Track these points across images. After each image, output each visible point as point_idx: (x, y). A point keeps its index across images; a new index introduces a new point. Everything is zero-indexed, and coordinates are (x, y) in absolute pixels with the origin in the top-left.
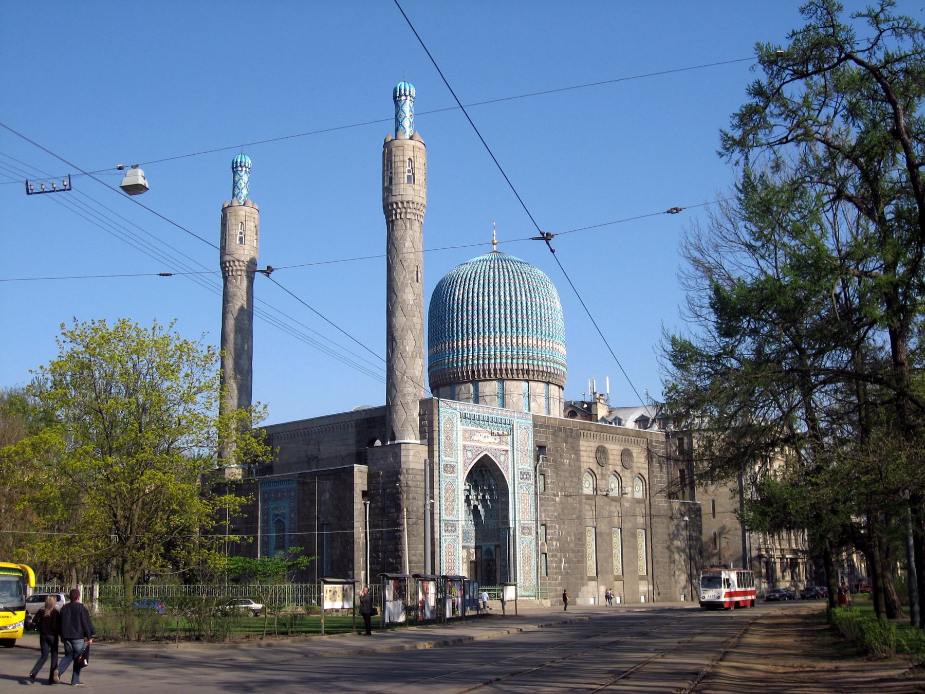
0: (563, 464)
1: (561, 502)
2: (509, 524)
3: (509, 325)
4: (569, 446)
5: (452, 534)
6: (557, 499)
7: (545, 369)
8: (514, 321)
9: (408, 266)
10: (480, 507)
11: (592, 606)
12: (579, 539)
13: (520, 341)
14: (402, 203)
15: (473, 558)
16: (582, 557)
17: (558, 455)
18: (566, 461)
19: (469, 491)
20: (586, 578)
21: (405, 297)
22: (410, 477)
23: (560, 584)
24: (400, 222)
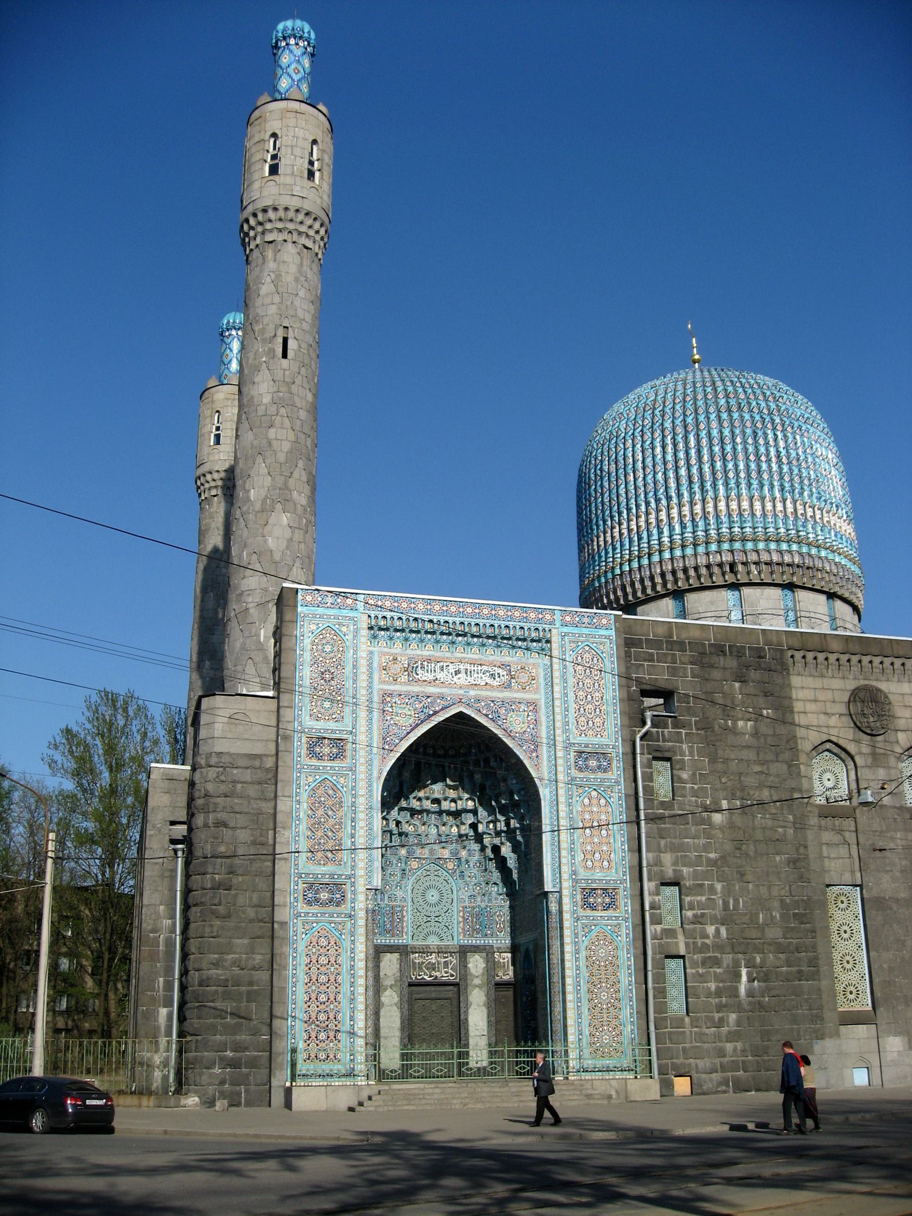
0: (734, 731)
1: (731, 826)
3: (684, 481)
4: (751, 688)
5: (331, 909)
6: (717, 818)
7: (775, 558)
8: (694, 470)
9: (263, 331)
10: (506, 850)
11: (860, 1089)
12: (801, 918)
13: (710, 508)
14: (255, 215)
15: (508, 974)
16: (813, 962)
17: (714, 712)
18: (745, 726)
19: (474, 812)
20: (827, 1015)
21: (254, 393)
22: (212, 773)
23: (733, 1037)
24: (256, 253)
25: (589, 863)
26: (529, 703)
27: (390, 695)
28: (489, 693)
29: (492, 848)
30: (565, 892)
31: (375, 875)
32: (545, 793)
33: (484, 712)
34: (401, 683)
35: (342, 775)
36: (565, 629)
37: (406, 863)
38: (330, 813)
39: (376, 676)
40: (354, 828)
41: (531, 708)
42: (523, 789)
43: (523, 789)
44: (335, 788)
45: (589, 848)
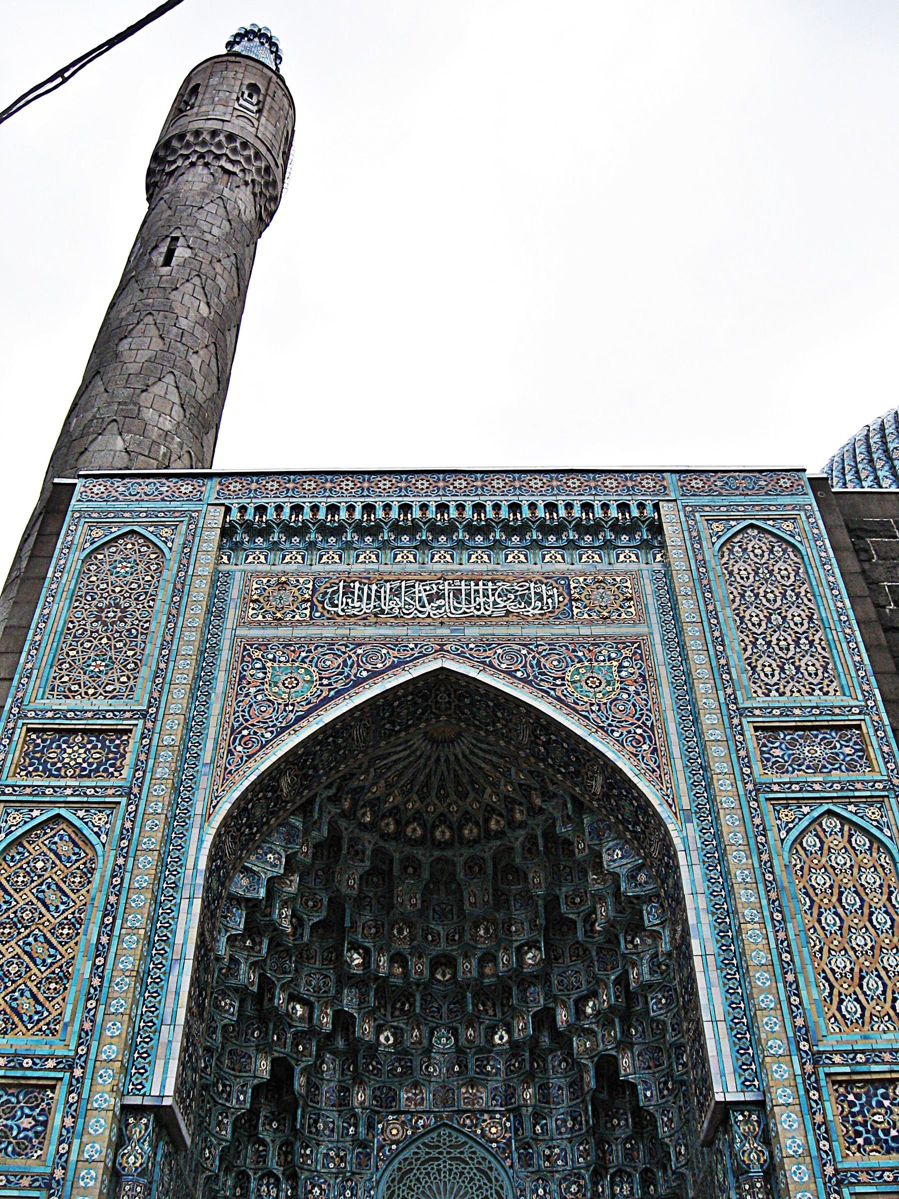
2: (705, 1082)
25: (850, 1005)
26: (620, 643)
27: (264, 646)
28: (515, 631)
29: (597, 1068)
30: (781, 1095)
31: (160, 1064)
32: (684, 836)
33: (504, 666)
34: (293, 624)
35: (102, 806)
36: (693, 501)
37: (371, 1127)
38: (52, 897)
39: (232, 615)
40: (107, 929)
41: (626, 653)
42: (639, 868)
43: (639, 868)
44: (79, 839)
45: (840, 962)
